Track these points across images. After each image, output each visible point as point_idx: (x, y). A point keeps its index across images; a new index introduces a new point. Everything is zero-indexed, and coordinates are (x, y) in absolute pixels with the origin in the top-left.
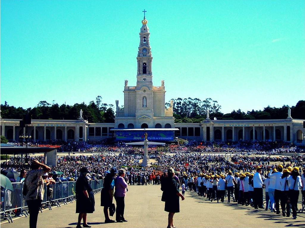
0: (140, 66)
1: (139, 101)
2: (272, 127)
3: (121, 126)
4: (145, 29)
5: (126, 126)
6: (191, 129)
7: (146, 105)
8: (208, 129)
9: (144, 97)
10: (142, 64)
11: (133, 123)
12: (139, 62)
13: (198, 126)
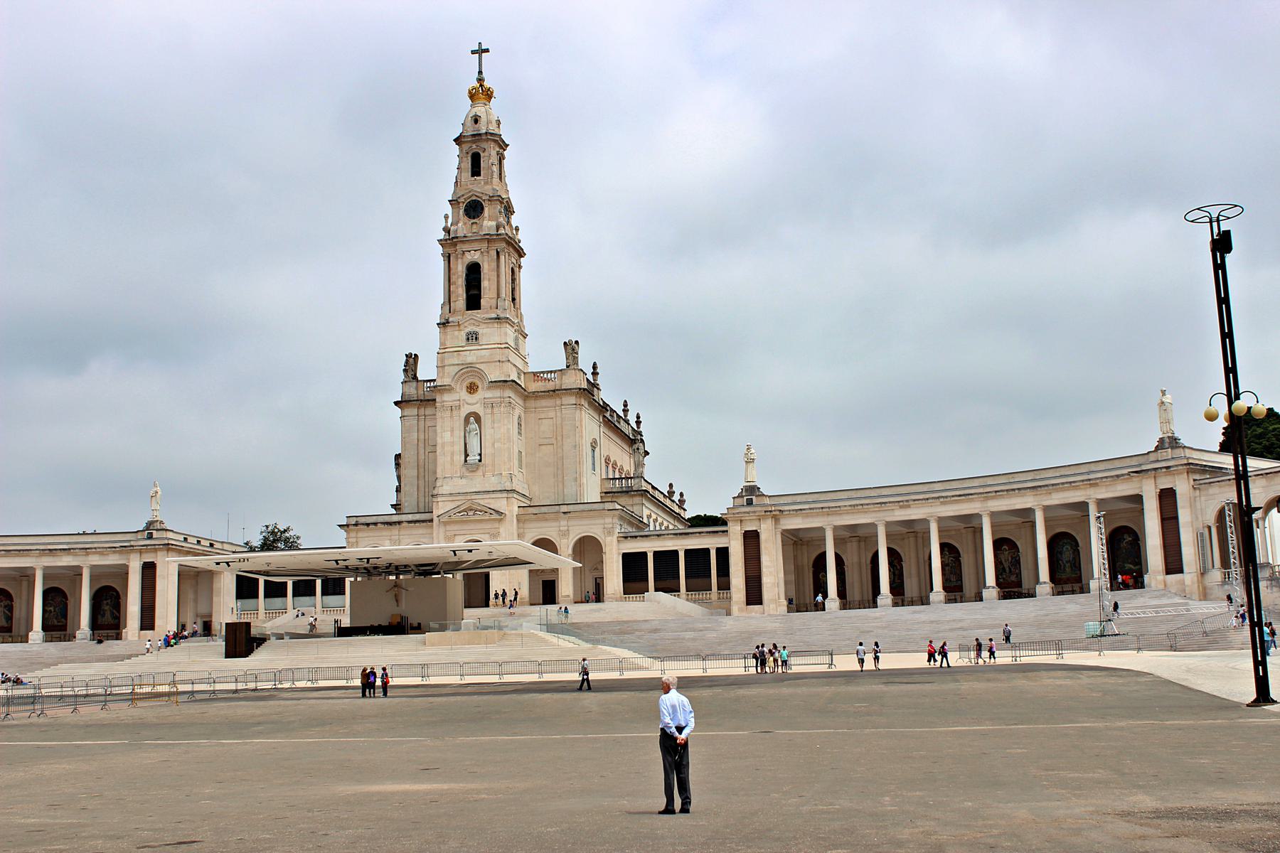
0: (453, 278)
1: (447, 435)
4: (476, 121)
7: (480, 455)
10: (460, 269)
12: (448, 258)
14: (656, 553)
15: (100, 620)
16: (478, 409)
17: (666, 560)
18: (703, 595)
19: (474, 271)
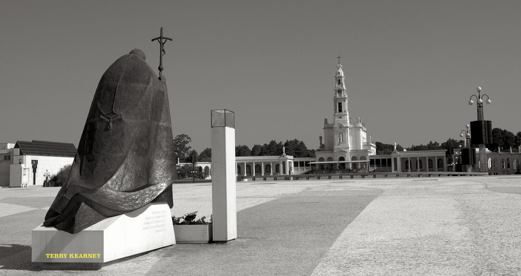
2: (425, 158)
3: (321, 159)
5: (359, 158)
6: (384, 161)
8: (395, 159)
9: (340, 133)
11: (331, 156)
13: (389, 158)
14: (376, 159)
15: (267, 171)
16: (341, 131)
17: (378, 161)
18: (385, 167)
19: (340, 104)
